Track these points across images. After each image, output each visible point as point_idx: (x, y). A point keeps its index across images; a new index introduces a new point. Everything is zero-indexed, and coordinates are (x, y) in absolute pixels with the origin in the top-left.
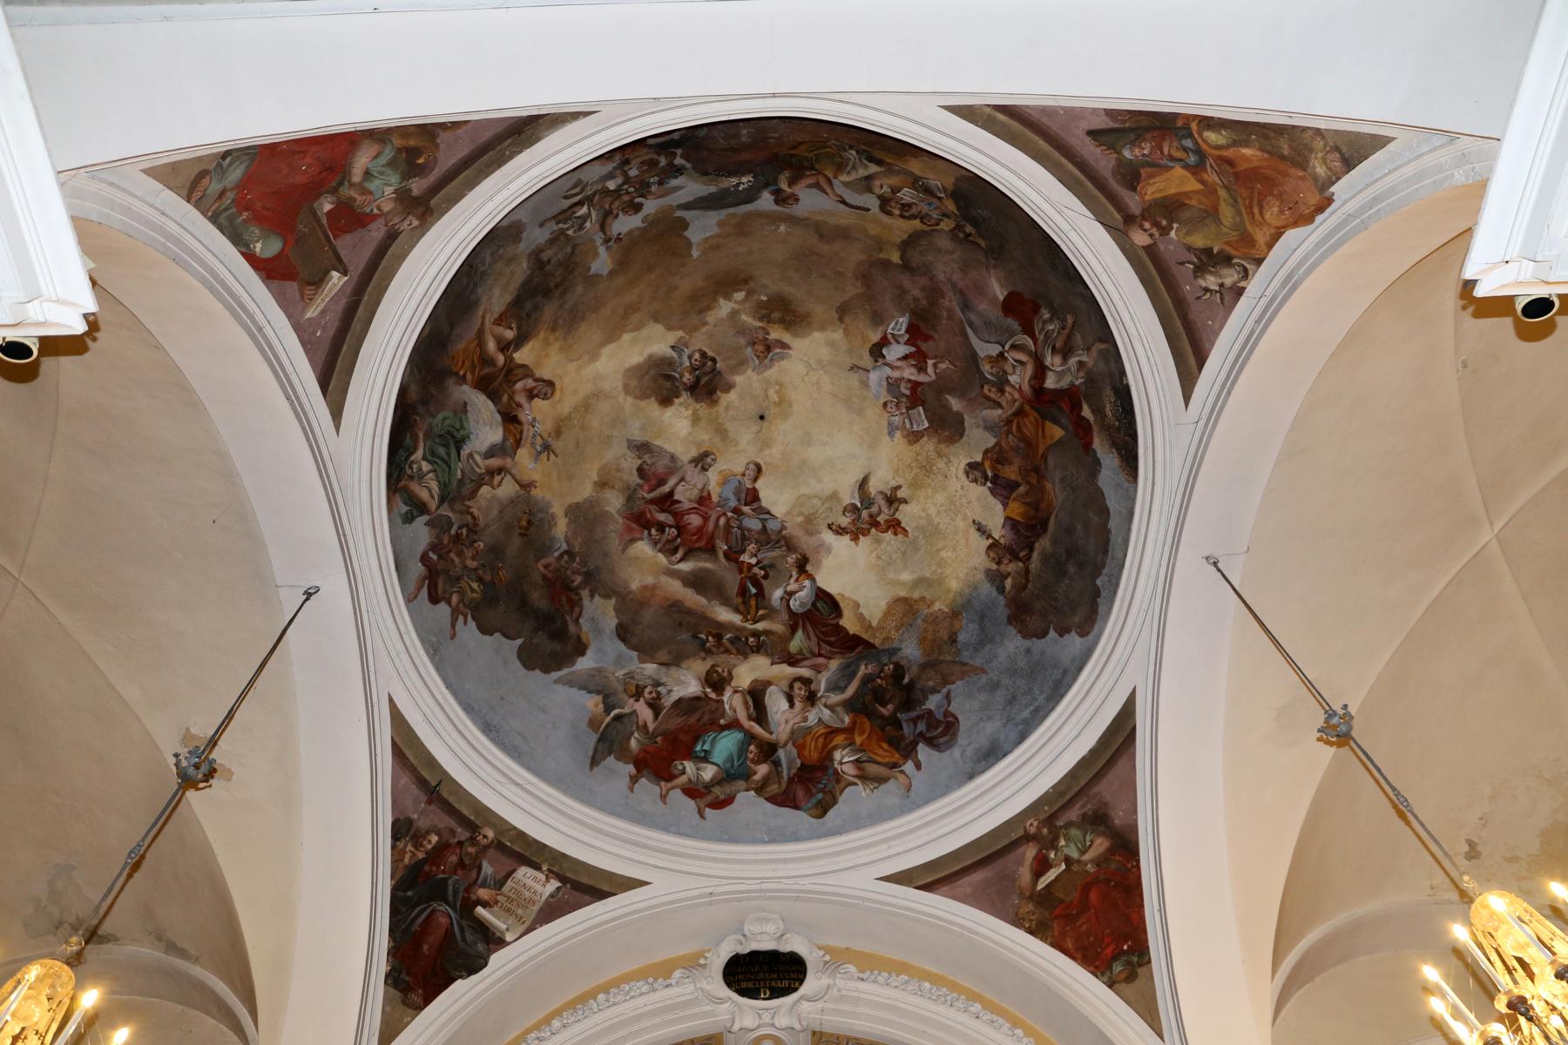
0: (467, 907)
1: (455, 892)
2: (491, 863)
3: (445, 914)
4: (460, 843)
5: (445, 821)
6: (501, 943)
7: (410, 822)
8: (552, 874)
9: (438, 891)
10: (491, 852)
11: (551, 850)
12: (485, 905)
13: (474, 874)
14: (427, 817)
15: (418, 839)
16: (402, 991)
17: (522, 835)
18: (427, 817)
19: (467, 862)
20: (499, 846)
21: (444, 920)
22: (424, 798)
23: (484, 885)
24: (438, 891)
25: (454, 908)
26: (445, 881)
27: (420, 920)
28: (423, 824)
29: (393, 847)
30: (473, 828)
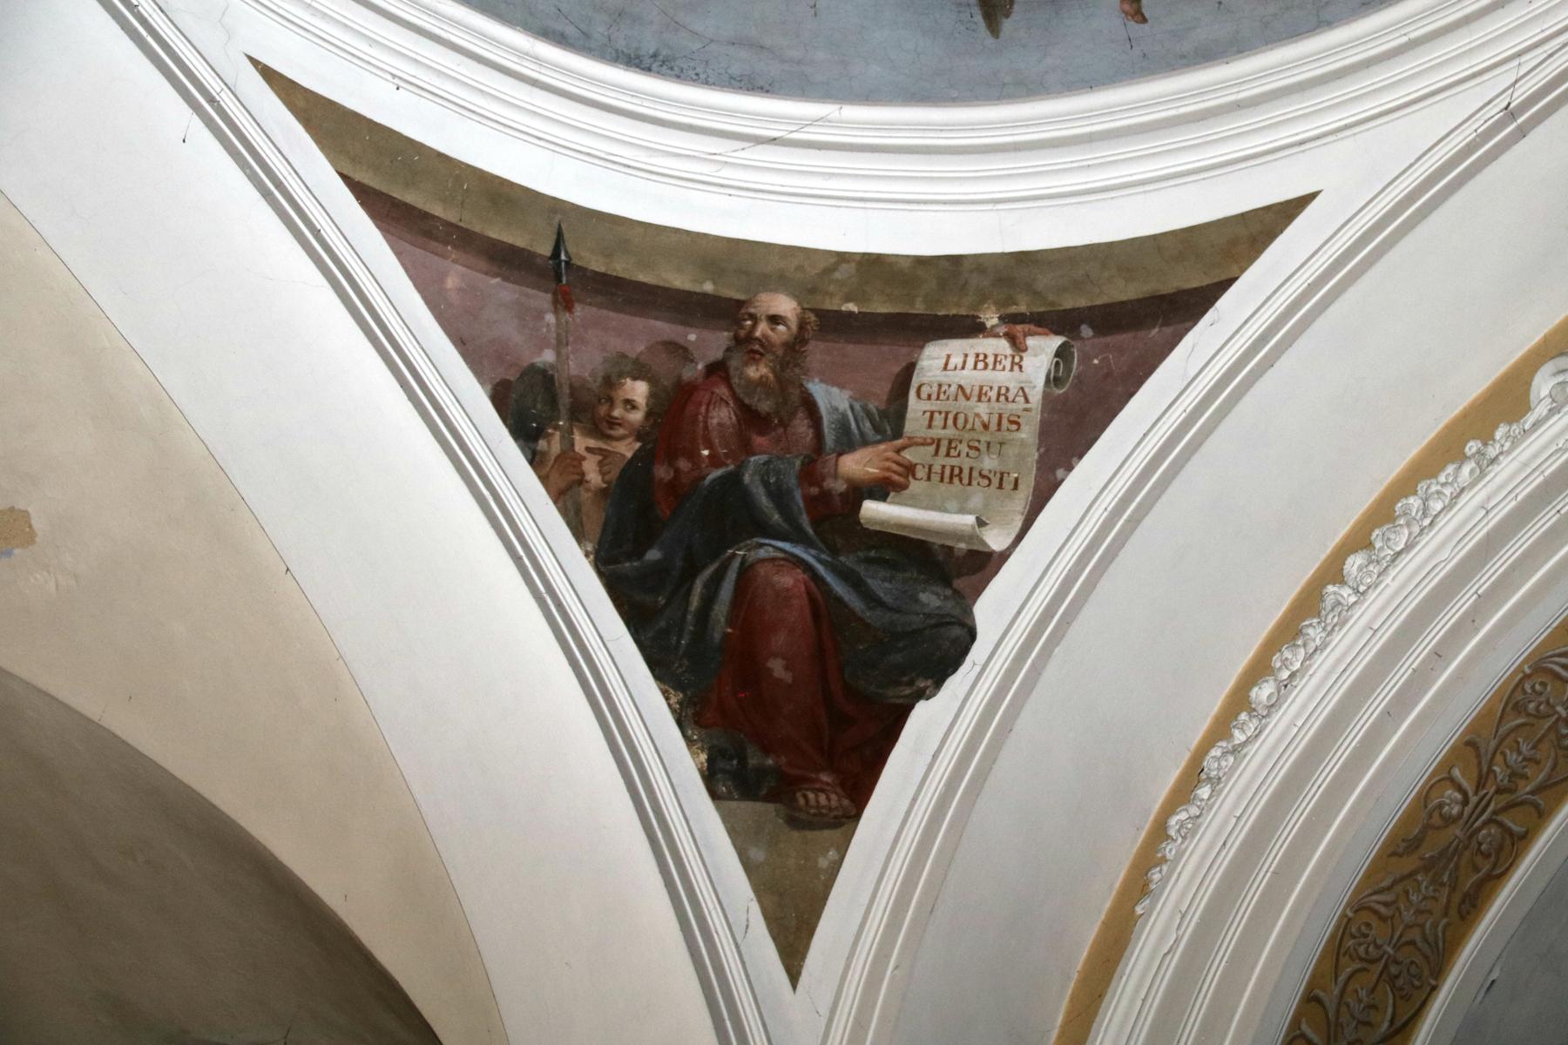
0: (835, 516)
1: (779, 496)
2: (829, 380)
3: (781, 564)
4: (717, 370)
5: (640, 334)
6: (984, 564)
7: (543, 379)
8: (1018, 326)
9: (729, 514)
10: (817, 352)
11: (979, 263)
12: (882, 489)
13: (801, 426)
14: (585, 346)
15: (591, 409)
16: (771, 798)
17: (873, 266)
18: (585, 346)
19: (765, 406)
20: (832, 325)
21: (788, 580)
22: (543, 300)
23: (848, 442)
24: (729, 514)
25: (798, 537)
26: (734, 480)
27: (721, 610)
28: (583, 365)
29: (535, 460)
30: (725, 312)
